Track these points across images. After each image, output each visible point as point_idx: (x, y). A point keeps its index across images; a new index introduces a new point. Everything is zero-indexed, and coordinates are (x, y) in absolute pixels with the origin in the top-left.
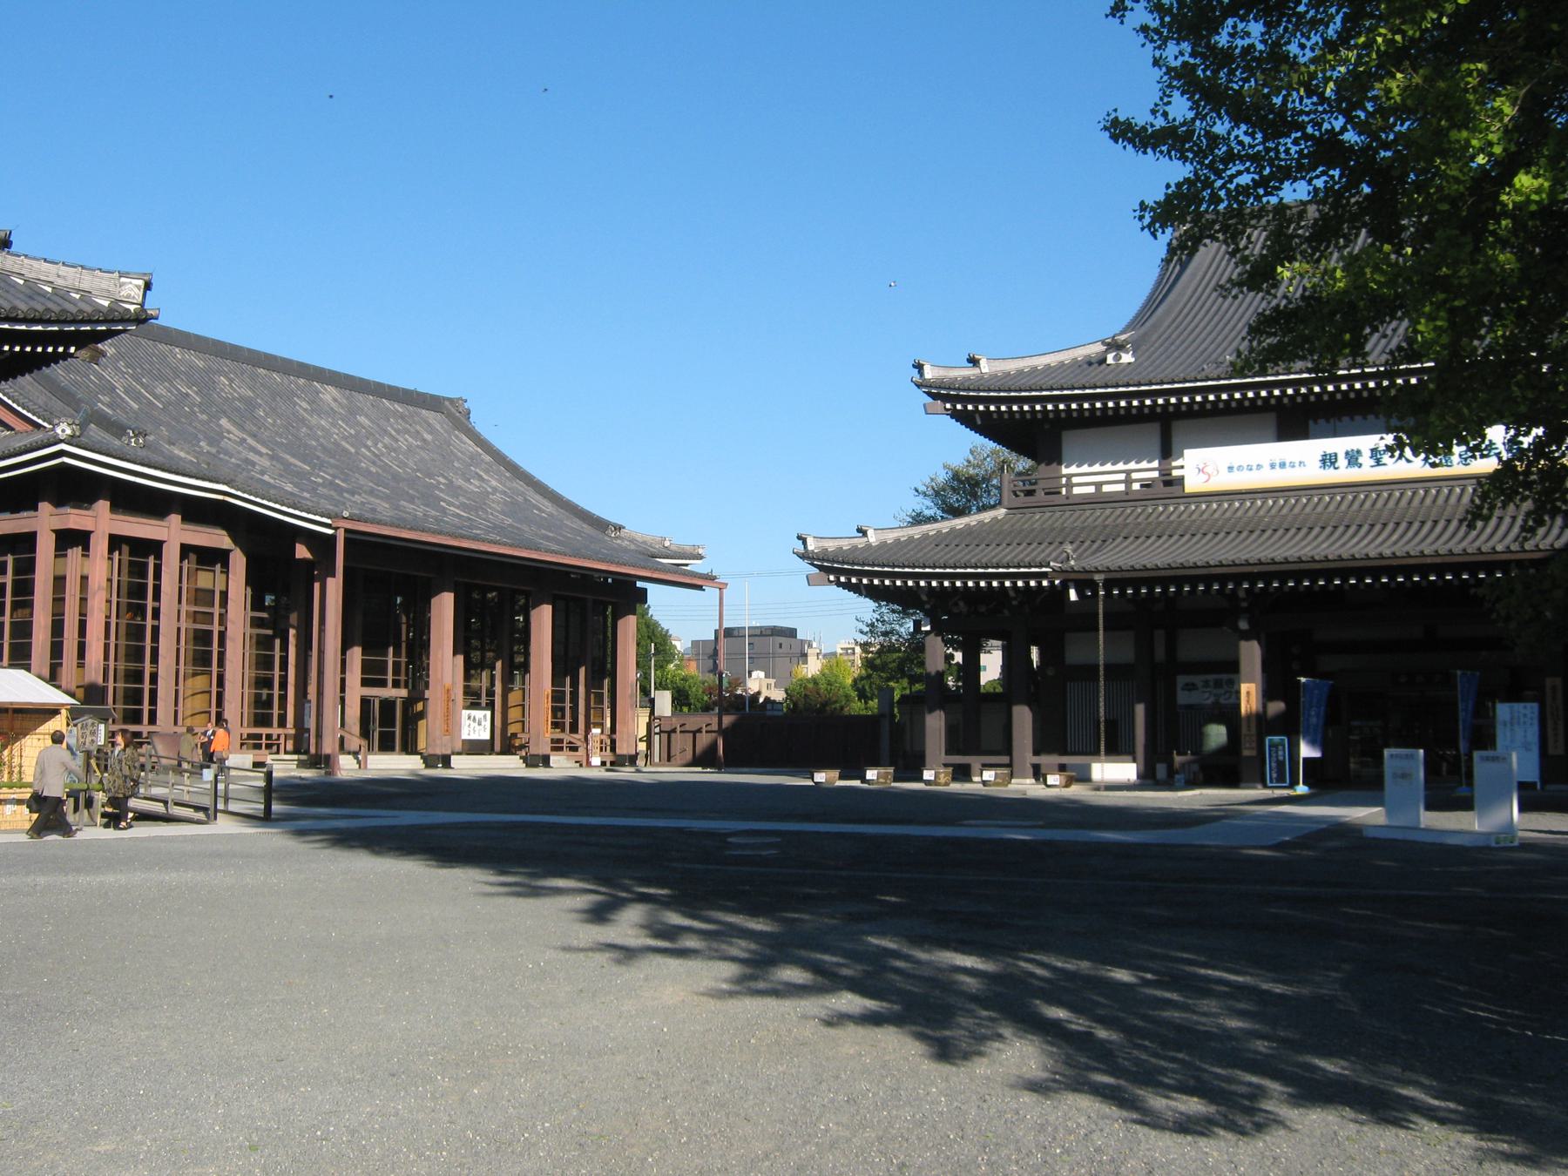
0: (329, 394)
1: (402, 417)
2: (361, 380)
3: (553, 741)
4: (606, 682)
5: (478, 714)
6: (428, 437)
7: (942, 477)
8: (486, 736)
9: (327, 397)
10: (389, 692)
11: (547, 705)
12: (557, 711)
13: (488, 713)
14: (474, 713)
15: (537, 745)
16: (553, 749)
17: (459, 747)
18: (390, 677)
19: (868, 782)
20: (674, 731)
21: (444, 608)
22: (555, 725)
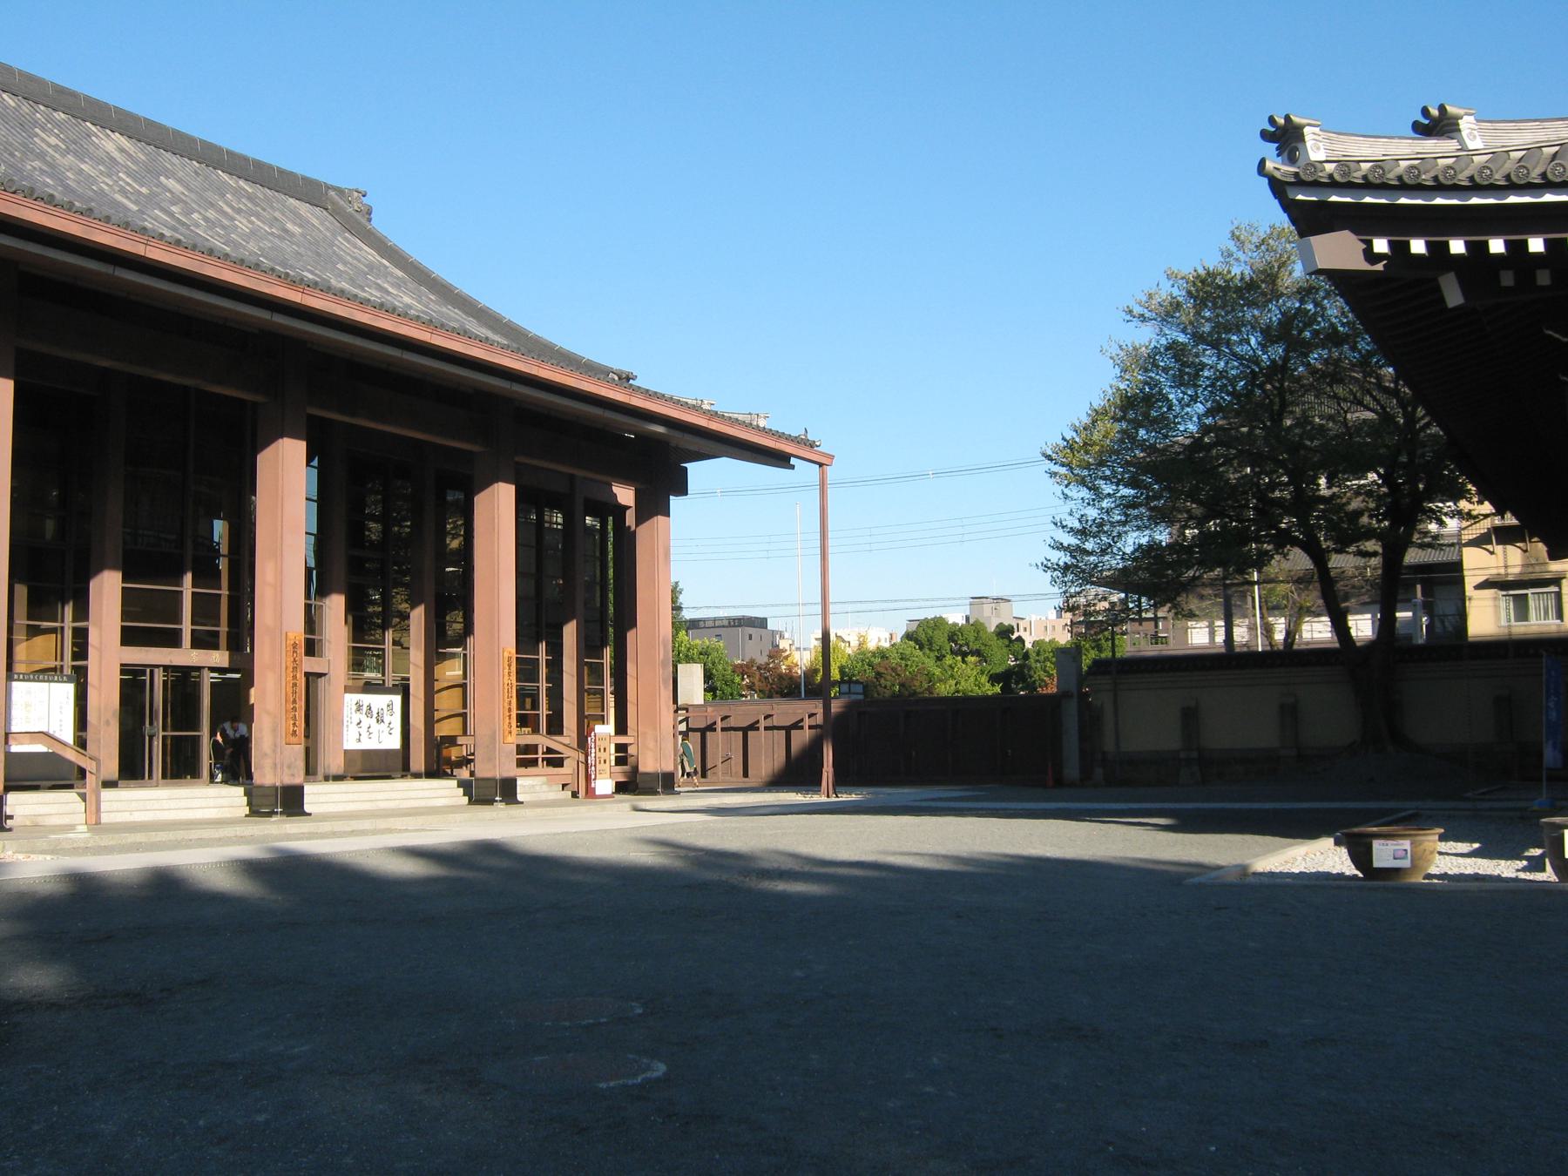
0: (112, 143)
1: (250, 198)
2: (177, 133)
3: (523, 749)
4: (608, 652)
5: (378, 701)
7: (1169, 291)
8: (394, 742)
9: (110, 147)
10: (186, 656)
11: (508, 679)
12: (526, 697)
15: (491, 759)
16: (522, 763)
17: (336, 764)
18: (187, 627)
20: (711, 728)
21: (286, 478)
22: (523, 721)
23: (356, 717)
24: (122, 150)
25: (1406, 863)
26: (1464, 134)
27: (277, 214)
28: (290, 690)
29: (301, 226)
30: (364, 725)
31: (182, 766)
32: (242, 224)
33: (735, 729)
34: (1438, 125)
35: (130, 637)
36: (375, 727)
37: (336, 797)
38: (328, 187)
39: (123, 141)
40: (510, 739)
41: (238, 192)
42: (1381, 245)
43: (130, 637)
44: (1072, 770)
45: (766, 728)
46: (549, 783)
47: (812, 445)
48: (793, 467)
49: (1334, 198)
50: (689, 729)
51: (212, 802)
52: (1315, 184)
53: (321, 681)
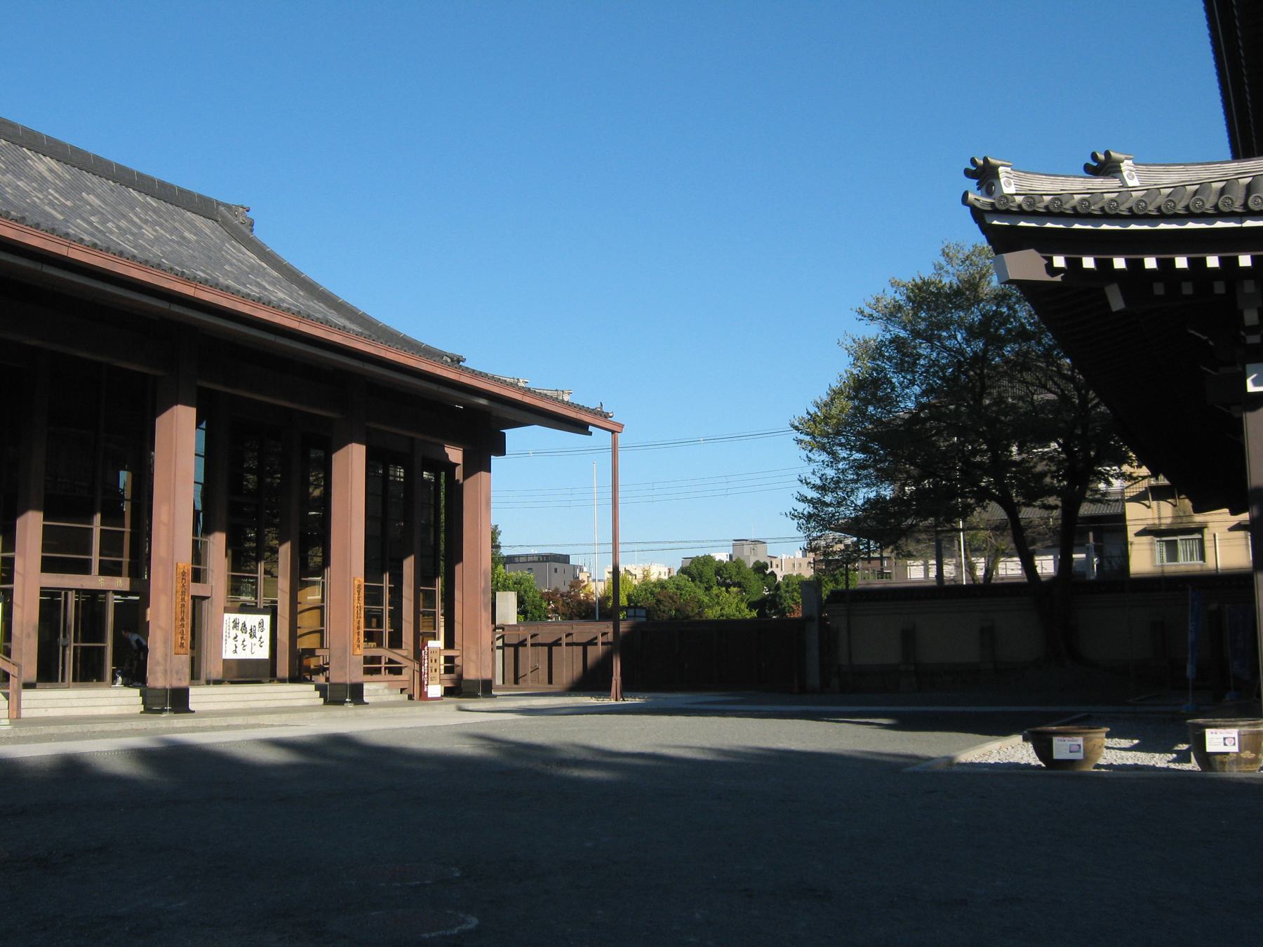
0: (43, 165)
1: (155, 211)
2: (97, 158)
3: (367, 660)
4: (439, 582)
5: (251, 620)
6: (192, 237)
7: (893, 296)
8: (263, 653)
9: (42, 168)
10: (94, 581)
11: (357, 602)
12: (372, 618)
13: (267, 619)
14: (242, 618)
16: (368, 671)
17: (216, 671)
18: (95, 558)
19: (1207, 760)
20: (523, 643)
21: (179, 439)
22: (369, 637)
23: (233, 633)
24: (51, 171)
25: (1079, 756)
26: (1125, 174)
27: (177, 224)
28: (179, 610)
29: (195, 234)
30: (240, 639)
31: (89, 672)
32: (148, 232)
33: (543, 645)
34: (1104, 167)
35: (48, 566)
36: (249, 641)
37: (216, 698)
38: (219, 204)
39: (53, 164)
40: (358, 652)
41: (145, 207)
42: (1059, 262)
43: (48, 566)
44: (814, 680)
45: (567, 644)
46: (389, 688)
47: (606, 416)
48: (590, 434)
49: (1022, 224)
50: (505, 645)
51: (113, 701)
52: (1007, 213)
53: (205, 603)
